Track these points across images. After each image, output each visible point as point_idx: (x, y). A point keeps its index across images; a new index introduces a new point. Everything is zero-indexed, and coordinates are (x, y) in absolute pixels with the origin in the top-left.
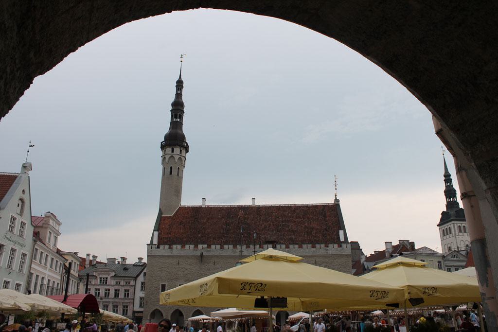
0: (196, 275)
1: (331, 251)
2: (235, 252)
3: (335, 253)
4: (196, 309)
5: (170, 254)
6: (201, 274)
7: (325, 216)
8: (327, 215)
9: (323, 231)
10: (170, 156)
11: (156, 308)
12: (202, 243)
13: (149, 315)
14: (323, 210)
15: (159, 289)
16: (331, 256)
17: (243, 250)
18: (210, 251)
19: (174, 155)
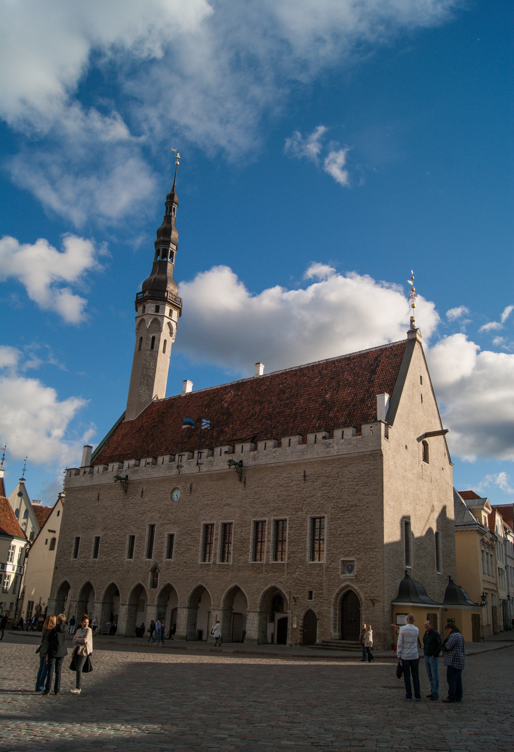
0: (117, 518)
1: (336, 447)
2: (170, 468)
3: (346, 451)
4: (111, 582)
5: (88, 483)
6: (123, 515)
7: (373, 372)
8: (379, 369)
9: (354, 405)
10: (140, 318)
11: (65, 580)
12: (128, 459)
13: (56, 592)
14: (376, 359)
15: (72, 547)
16: (338, 459)
17: (183, 464)
18: (136, 472)
19: (145, 317)
